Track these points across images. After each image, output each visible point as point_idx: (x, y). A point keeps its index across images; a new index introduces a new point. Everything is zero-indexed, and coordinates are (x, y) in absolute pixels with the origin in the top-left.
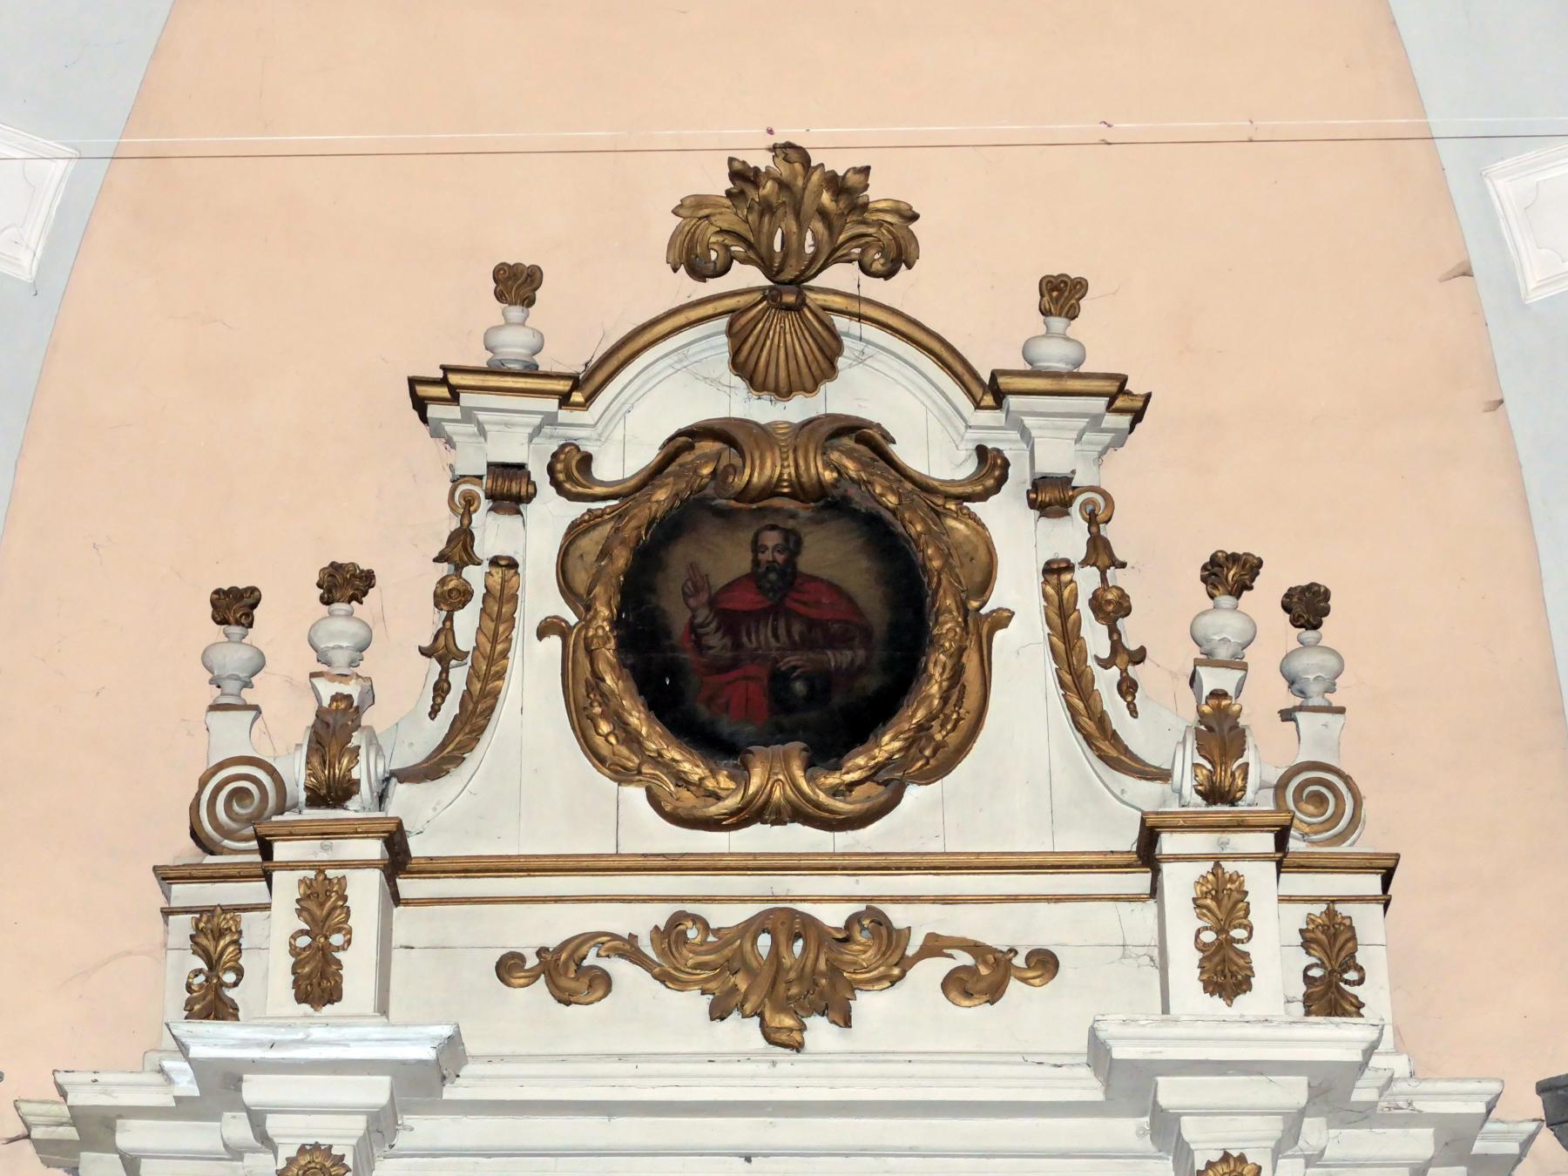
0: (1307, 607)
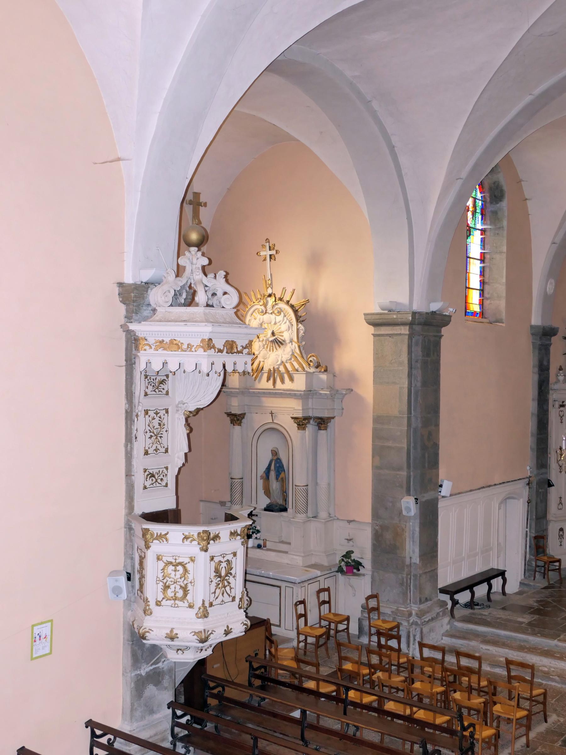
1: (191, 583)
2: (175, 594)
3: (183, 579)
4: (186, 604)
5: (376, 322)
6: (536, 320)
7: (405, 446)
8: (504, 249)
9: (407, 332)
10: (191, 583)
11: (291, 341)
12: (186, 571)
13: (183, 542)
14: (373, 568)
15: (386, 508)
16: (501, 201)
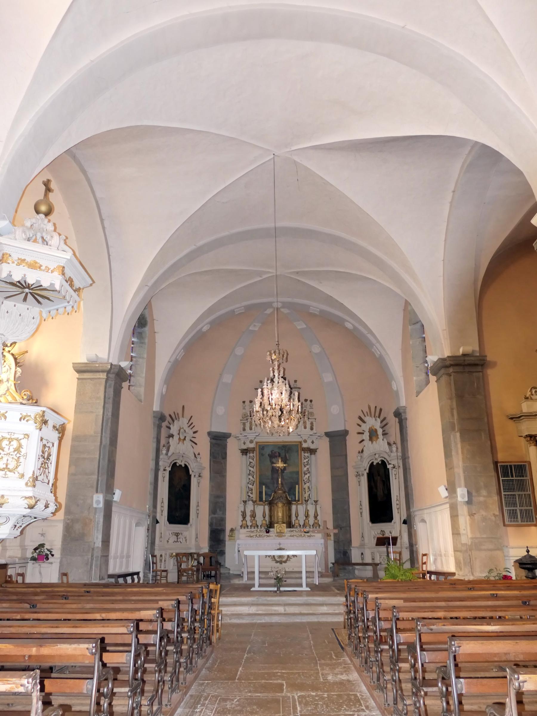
0: (311, 401)
1: (24, 456)
2: (7, 466)
3: (16, 452)
4: (17, 475)
5: (81, 370)
6: (156, 407)
7: (97, 456)
8: (145, 356)
9: (105, 377)
10: (24, 456)
11: (8, 381)
12: (20, 446)
13: (20, 420)
14: (61, 554)
15: (78, 505)
16: (145, 327)
